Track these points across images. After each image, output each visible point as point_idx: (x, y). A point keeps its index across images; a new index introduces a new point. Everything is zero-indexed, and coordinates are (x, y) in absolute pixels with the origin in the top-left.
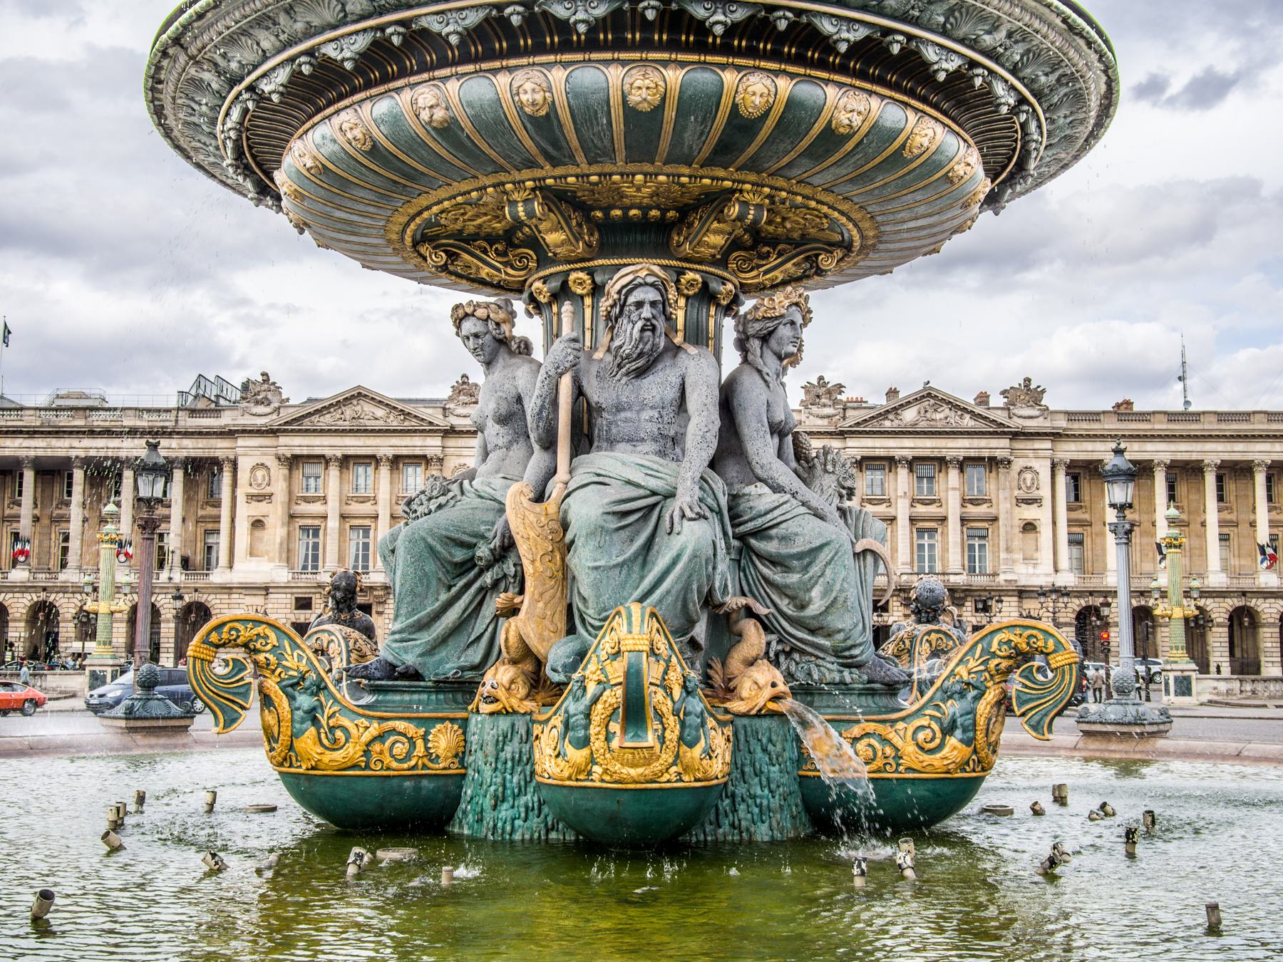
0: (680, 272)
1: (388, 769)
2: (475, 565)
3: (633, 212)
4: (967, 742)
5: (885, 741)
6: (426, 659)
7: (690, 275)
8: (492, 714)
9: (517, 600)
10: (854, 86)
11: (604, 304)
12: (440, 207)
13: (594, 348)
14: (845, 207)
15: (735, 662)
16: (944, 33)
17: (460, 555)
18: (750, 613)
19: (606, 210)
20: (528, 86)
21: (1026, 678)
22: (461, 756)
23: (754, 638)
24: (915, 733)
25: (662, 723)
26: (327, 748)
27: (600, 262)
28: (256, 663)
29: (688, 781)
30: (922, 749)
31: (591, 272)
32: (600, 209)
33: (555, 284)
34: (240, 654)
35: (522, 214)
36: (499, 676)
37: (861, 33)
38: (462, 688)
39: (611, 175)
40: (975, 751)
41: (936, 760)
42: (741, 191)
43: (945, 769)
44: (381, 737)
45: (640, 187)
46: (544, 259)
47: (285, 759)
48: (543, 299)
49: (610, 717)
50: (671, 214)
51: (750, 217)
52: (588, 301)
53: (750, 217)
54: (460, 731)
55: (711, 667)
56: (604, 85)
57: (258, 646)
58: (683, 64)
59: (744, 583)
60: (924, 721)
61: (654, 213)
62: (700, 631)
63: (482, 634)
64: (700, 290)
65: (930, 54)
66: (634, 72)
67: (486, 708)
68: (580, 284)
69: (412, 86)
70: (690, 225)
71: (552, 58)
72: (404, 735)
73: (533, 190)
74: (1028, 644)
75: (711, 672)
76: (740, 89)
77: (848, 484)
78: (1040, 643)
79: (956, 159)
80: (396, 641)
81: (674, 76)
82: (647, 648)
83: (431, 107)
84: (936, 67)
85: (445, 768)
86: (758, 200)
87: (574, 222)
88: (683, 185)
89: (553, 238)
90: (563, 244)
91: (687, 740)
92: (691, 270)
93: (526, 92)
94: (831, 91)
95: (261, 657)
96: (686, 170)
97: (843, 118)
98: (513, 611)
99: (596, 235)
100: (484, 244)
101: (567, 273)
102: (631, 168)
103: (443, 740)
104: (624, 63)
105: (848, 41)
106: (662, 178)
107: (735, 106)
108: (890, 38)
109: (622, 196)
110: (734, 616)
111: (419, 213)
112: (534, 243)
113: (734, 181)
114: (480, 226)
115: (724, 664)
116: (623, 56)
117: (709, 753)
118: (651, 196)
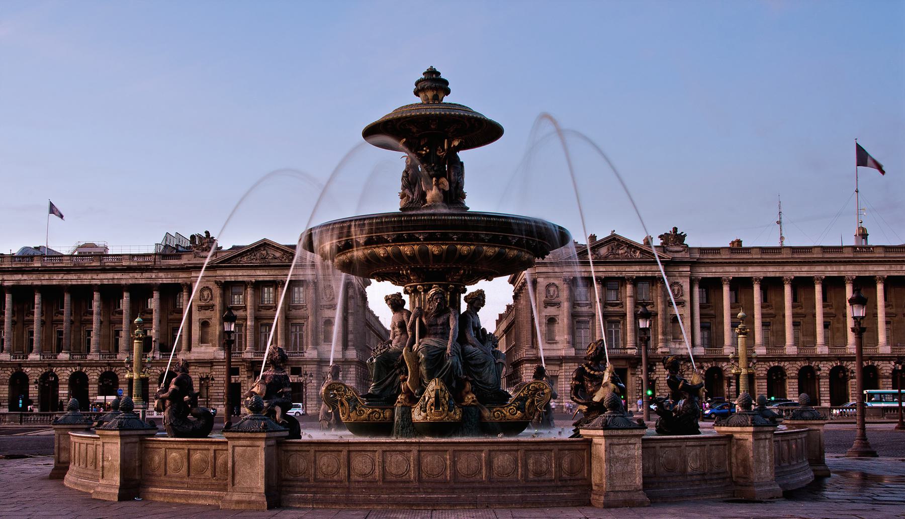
5: (502, 412)
11: (428, 297)
23: (468, 386)
29: (450, 420)
41: (515, 417)
44: (372, 413)
49: (432, 405)
58: (446, 244)
62: (454, 385)
91: (450, 410)
117: (455, 413)
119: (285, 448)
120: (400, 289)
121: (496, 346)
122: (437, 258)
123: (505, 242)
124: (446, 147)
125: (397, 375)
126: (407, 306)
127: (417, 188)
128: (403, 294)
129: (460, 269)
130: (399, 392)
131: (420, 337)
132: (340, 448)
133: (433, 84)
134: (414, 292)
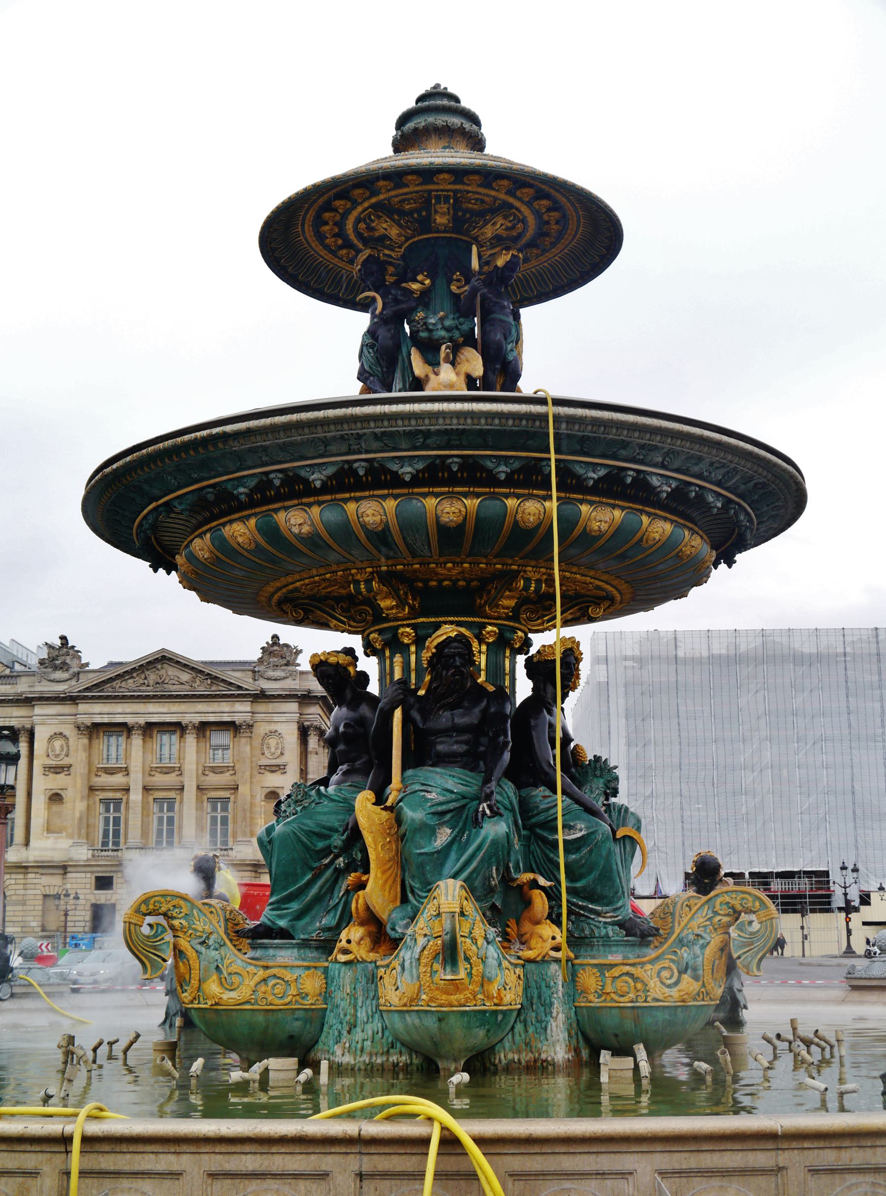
0: (483, 626)
1: (271, 1004)
2: (331, 852)
3: (446, 583)
4: (696, 978)
5: (635, 979)
6: (295, 922)
7: (489, 628)
8: (346, 963)
9: (364, 878)
10: (602, 502)
11: (426, 655)
12: (302, 582)
13: (418, 689)
14: (605, 578)
16: (663, 466)
17: (320, 845)
18: (534, 884)
19: (426, 582)
20: (369, 512)
21: (741, 930)
24: (659, 973)
25: (470, 964)
26: (226, 989)
27: (422, 620)
28: (172, 928)
30: (663, 983)
31: (414, 627)
32: (421, 581)
33: (388, 636)
34: (161, 920)
35: (363, 590)
37: (602, 472)
39: (429, 564)
40: (704, 985)
42: (525, 572)
43: (680, 999)
44: (265, 980)
45: (450, 570)
46: (378, 616)
47: (195, 998)
48: (378, 646)
49: (435, 957)
50: (474, 583)
51: (532, 588)
52: (413, 649)
53: (532, 588)
54: (323, 976)
55: (508, 926)
56: (423, 510)
57: (175, 915)
58: (478, 495)
59: (533, 862)
60: (667, 964)
61: (461, 583)
63: (338, 904)
64: (497, 638)
65: (655, 481)
66: (444, 501)
67: (343, 958)
68: (407, 636)
69: (286, 508)
70: (489, 592)
71: (386, 492)
72: (283, 979)
73: (372, 573)
74: (741, 904)
75: (509, 930)
76: (519, 511)
77: (612, 785)
78: (750, 904)
79: (683, 544)
80: (272, 910)
81: (472, 503)
82: (458, 910)
83: (300, 525)
84: (659, 489)
85: (312, 1004)
86: (537, 576)
87: (402, 592)
88: (481, 568)
89: (385, 603)
90: (392, 608)
92: (491, 624)
93: (368, 516)
94: (584, 508)
95: (176, 923)
96: (484, 560)
97: (595, 526)
98: (362, 886)
99: (418, 599)
100: (332, 603)
101: (397, 628)
102: (442, 560)
103: (312, 984)
104: (436, 495)
105: (593, 479)
106: (466, 565)
107: (516, 522)
108: (623, 474)
109: (437, 574)
110: (525, 888)
111: (287, 585)
112: (371, 602)
113: (519, 566)
114: (330, 592)
115: (518, 924)
116: (436, 490)
118: (459, 573)
120: (356, 642)
121: (615, 793)
122: (450, 536)
123: (638, 494)
124: (475, 264)
125: (339, 874)
126: (373, 688)
127: (398, 375)
128: (360, 652)
129: (515, 575)
130: (346, 918)
131: (404, 768)
132: (29, 1160)
133: (437, 116)
134: (384, 646)
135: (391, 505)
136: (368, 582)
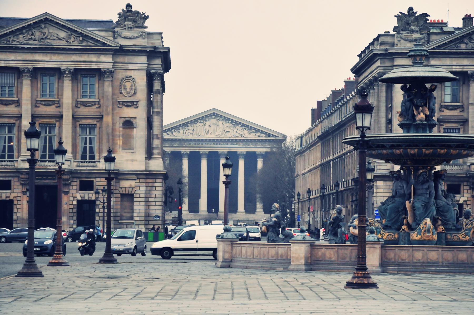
15: (437, 225)
18: (438, 218)
22: (398, 238)
23: (440, 222)
36: (404, 227)
38: (399, 229)
44: (388, 235)
103: (396, 236)
119: (384, 248)
122: (426, 155)
135: (416, 150)
136: (407, 160)
